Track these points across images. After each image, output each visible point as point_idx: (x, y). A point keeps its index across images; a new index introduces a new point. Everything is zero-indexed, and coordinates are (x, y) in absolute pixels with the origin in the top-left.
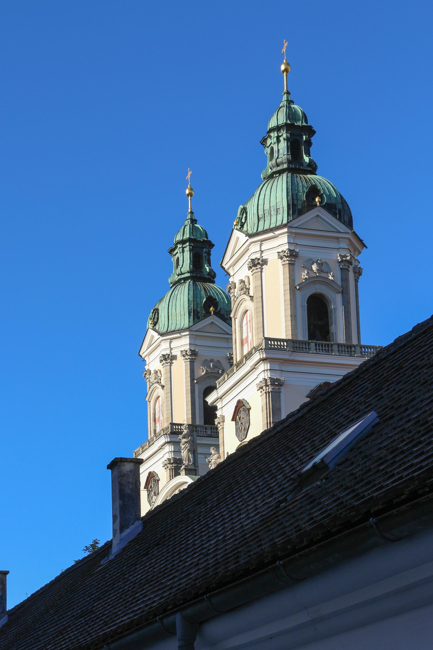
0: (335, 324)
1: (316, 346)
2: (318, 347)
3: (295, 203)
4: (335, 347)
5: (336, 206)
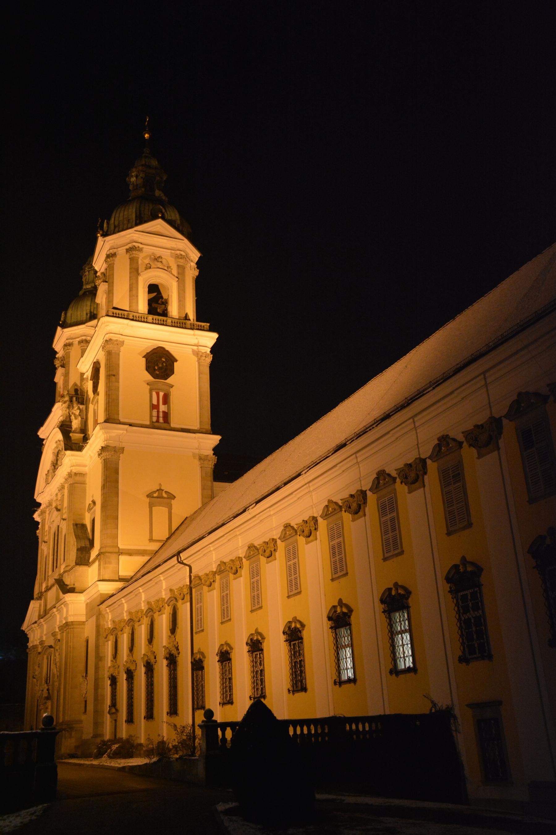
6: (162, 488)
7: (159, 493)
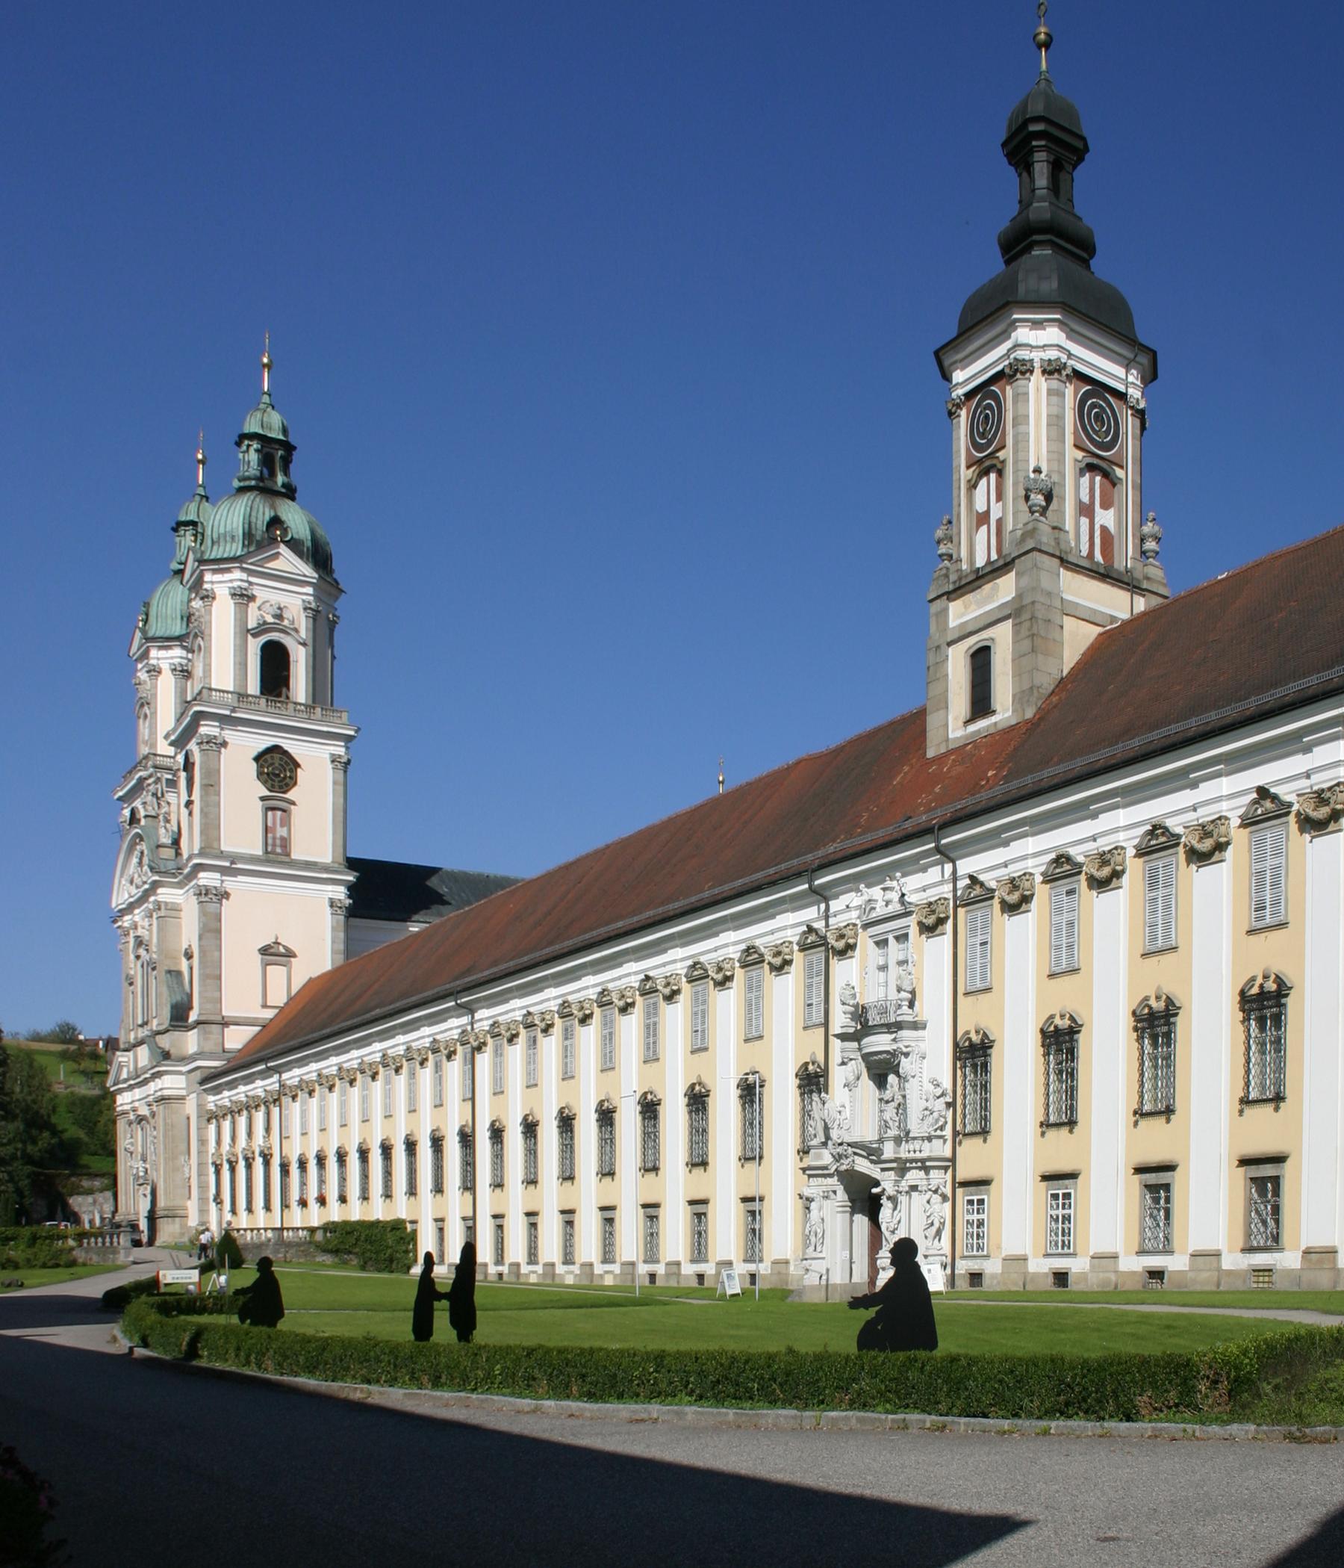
1: (267, 701)
3: (253, 532)
6: (279, 941)
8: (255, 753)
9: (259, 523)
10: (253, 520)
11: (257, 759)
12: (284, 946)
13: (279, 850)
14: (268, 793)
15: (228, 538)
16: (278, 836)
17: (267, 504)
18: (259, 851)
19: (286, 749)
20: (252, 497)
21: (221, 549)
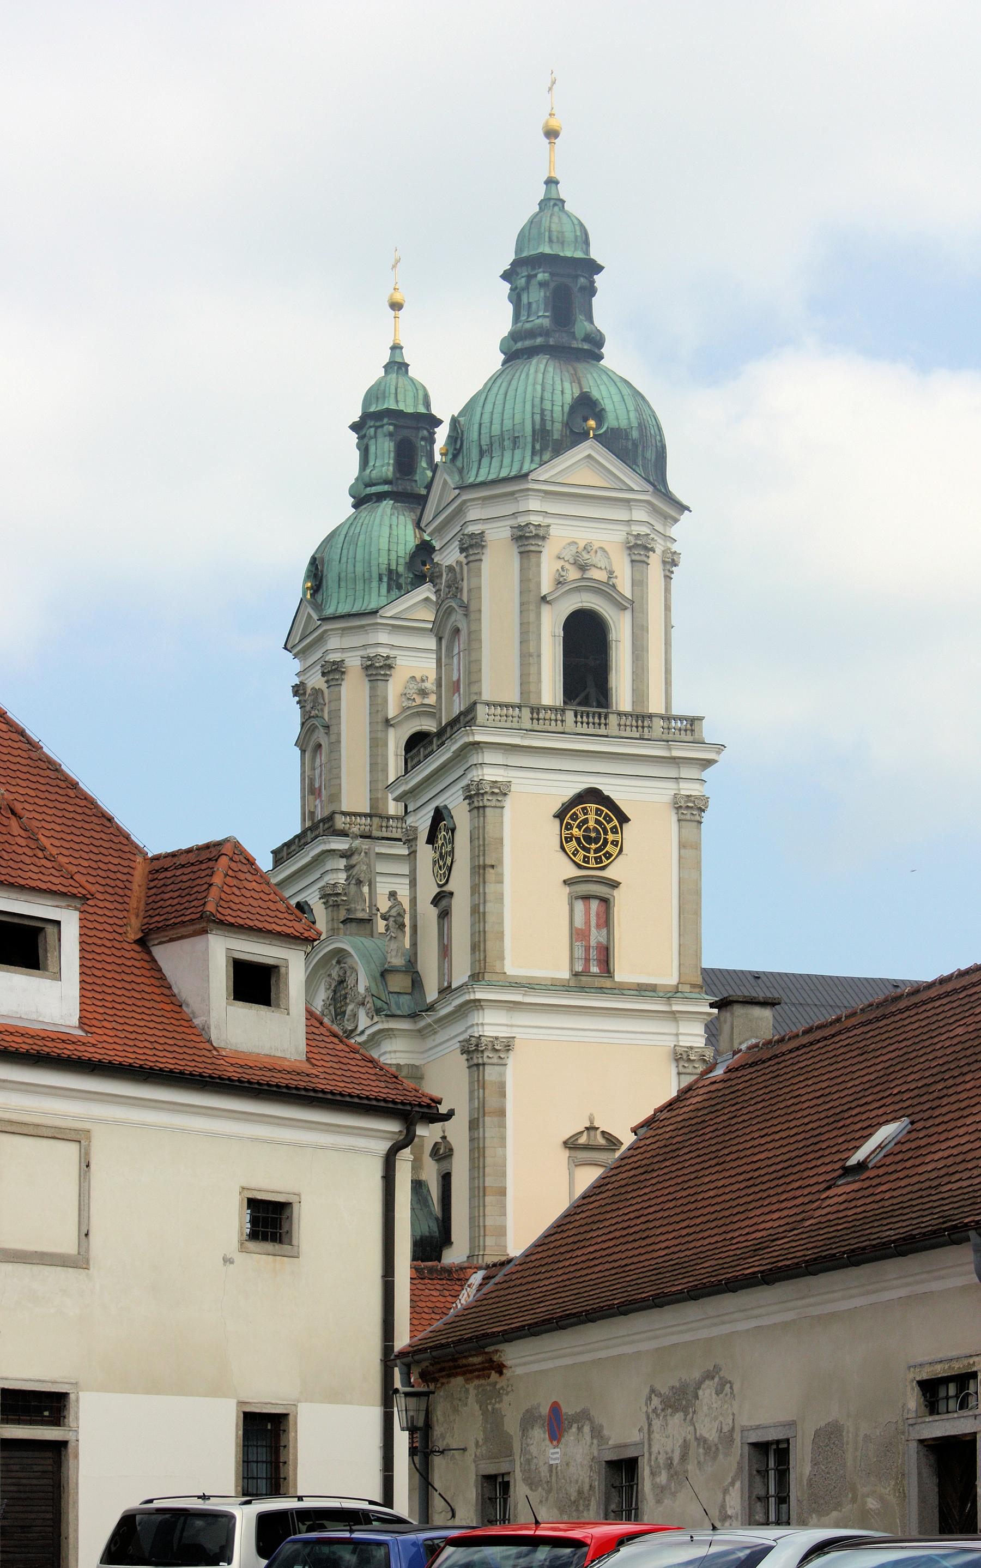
0: (616, 670)
2: (579, 719)
3: (549, 428)
4: (613, 719)
5: (627, 435)
7: (589, 1135)
8: (556, 806)
9: (557, 409)
10: (547, 405)
11: (560, 816)
12: (603, 1132)
13: (595, 969)
14: (574, 872)
15: (506, 443)
16: (593, 943)
17: (566, 375)
18: (565, 975)
19: (606, 793)
20: (542, 367)
21: (496, 462)
